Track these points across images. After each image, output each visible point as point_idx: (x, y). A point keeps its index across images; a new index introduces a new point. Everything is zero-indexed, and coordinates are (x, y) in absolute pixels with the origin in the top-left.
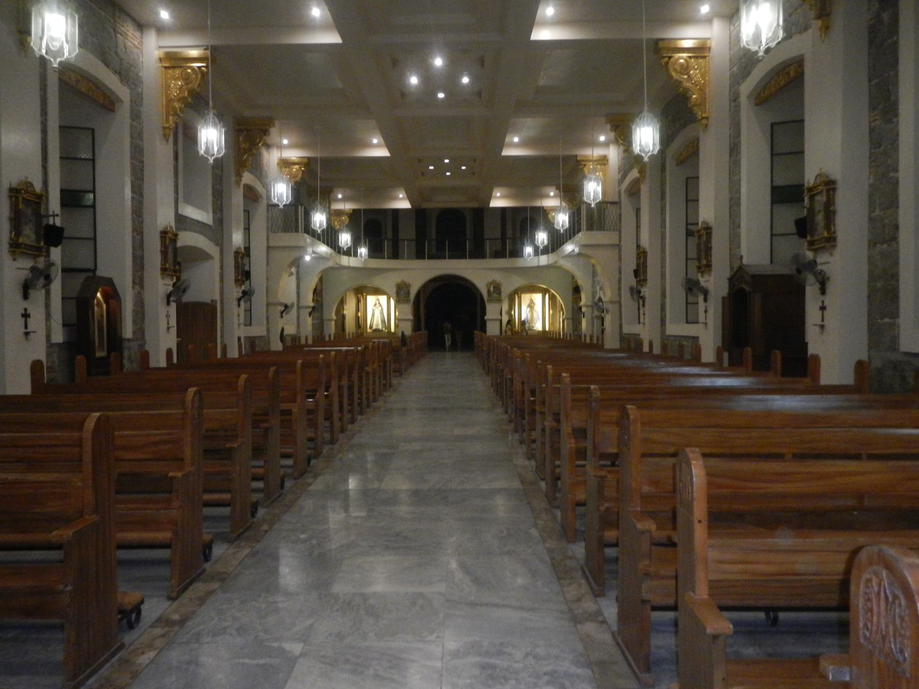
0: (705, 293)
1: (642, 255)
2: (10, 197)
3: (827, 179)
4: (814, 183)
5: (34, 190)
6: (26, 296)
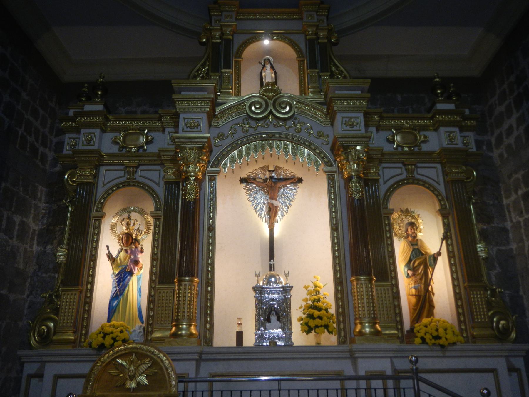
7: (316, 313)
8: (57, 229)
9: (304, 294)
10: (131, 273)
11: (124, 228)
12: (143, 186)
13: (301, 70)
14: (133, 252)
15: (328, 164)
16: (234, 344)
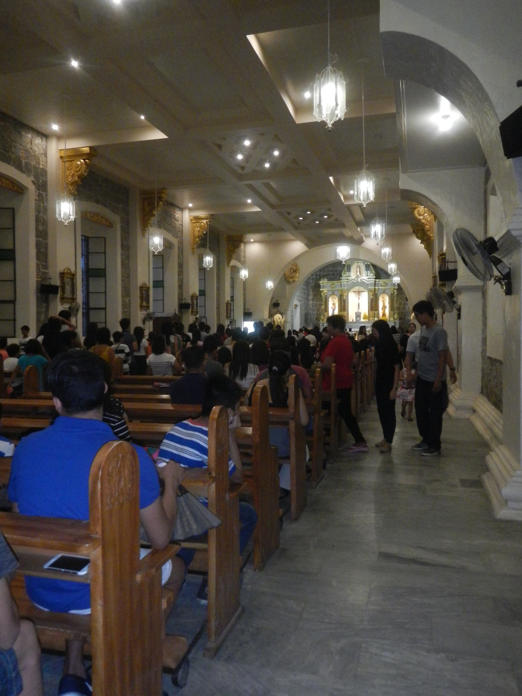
2: (140, 290)
8: (316, 298)
9: (364, 313)
14: (335, 307)
15: (368, 291)
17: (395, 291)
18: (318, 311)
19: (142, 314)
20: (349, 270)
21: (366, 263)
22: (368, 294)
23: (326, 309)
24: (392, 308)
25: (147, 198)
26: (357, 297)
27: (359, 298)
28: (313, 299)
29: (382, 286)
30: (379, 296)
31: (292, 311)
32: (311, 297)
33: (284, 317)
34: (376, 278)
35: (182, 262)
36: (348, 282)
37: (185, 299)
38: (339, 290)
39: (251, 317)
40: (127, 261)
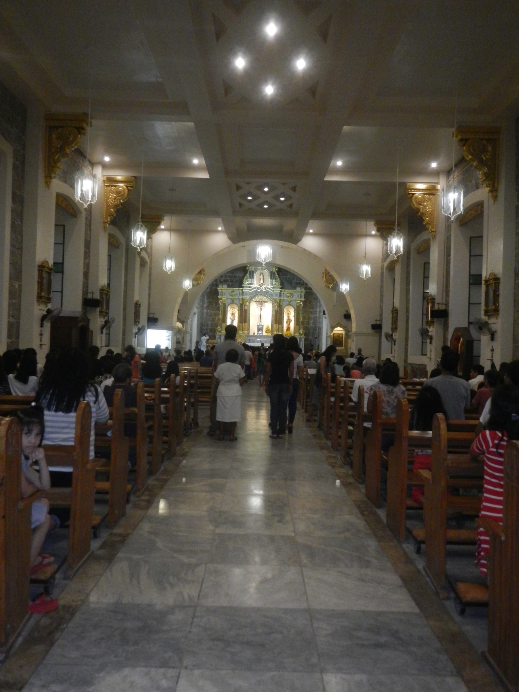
0: (431, 338)
1: (395, 312)
2: (39, 270)
3: (495, 277)
4: (489, 278)
5: (49, 266)
6: (42, 325)
7: (268, 330)
10: (234, 321)
11: (232, 312)
12: (235, 304)
13: (269, 278)
14: (234, 317)
15: (273, 302)
16: (253, 334)
17: (301, 303)
18: (213, 321)
19: (40, 310)
20: (252, 277)
21: (271, 270)
22: (273, 305)
23: (224, 319)
24: (297, 322)
25: (57, 127)
26: (259, 307)
27: (261, 309)
28: (208, 308)
29: (288, 297)
30: (285, 307)
31: (192, 319)
32: (205, 305)
33: (184, 327)
34: (282, 288)
35: (89, 239)
36: (250, 290)
37: (93, 293)
38: (240, 299)
39: (156, 324)
40: (19, 222)
